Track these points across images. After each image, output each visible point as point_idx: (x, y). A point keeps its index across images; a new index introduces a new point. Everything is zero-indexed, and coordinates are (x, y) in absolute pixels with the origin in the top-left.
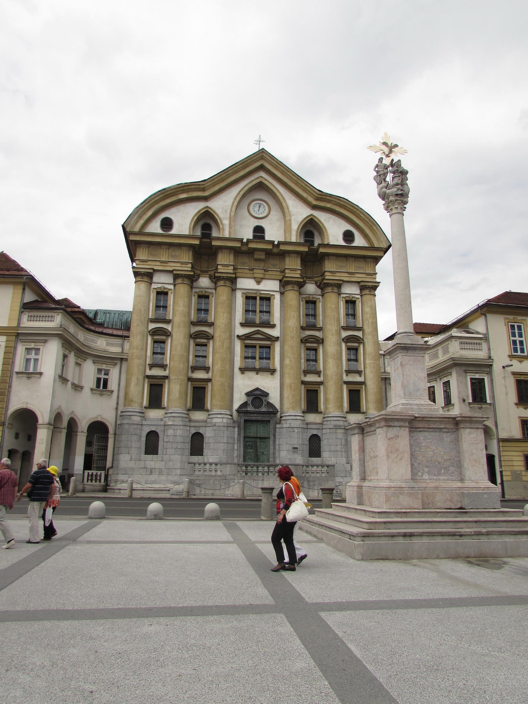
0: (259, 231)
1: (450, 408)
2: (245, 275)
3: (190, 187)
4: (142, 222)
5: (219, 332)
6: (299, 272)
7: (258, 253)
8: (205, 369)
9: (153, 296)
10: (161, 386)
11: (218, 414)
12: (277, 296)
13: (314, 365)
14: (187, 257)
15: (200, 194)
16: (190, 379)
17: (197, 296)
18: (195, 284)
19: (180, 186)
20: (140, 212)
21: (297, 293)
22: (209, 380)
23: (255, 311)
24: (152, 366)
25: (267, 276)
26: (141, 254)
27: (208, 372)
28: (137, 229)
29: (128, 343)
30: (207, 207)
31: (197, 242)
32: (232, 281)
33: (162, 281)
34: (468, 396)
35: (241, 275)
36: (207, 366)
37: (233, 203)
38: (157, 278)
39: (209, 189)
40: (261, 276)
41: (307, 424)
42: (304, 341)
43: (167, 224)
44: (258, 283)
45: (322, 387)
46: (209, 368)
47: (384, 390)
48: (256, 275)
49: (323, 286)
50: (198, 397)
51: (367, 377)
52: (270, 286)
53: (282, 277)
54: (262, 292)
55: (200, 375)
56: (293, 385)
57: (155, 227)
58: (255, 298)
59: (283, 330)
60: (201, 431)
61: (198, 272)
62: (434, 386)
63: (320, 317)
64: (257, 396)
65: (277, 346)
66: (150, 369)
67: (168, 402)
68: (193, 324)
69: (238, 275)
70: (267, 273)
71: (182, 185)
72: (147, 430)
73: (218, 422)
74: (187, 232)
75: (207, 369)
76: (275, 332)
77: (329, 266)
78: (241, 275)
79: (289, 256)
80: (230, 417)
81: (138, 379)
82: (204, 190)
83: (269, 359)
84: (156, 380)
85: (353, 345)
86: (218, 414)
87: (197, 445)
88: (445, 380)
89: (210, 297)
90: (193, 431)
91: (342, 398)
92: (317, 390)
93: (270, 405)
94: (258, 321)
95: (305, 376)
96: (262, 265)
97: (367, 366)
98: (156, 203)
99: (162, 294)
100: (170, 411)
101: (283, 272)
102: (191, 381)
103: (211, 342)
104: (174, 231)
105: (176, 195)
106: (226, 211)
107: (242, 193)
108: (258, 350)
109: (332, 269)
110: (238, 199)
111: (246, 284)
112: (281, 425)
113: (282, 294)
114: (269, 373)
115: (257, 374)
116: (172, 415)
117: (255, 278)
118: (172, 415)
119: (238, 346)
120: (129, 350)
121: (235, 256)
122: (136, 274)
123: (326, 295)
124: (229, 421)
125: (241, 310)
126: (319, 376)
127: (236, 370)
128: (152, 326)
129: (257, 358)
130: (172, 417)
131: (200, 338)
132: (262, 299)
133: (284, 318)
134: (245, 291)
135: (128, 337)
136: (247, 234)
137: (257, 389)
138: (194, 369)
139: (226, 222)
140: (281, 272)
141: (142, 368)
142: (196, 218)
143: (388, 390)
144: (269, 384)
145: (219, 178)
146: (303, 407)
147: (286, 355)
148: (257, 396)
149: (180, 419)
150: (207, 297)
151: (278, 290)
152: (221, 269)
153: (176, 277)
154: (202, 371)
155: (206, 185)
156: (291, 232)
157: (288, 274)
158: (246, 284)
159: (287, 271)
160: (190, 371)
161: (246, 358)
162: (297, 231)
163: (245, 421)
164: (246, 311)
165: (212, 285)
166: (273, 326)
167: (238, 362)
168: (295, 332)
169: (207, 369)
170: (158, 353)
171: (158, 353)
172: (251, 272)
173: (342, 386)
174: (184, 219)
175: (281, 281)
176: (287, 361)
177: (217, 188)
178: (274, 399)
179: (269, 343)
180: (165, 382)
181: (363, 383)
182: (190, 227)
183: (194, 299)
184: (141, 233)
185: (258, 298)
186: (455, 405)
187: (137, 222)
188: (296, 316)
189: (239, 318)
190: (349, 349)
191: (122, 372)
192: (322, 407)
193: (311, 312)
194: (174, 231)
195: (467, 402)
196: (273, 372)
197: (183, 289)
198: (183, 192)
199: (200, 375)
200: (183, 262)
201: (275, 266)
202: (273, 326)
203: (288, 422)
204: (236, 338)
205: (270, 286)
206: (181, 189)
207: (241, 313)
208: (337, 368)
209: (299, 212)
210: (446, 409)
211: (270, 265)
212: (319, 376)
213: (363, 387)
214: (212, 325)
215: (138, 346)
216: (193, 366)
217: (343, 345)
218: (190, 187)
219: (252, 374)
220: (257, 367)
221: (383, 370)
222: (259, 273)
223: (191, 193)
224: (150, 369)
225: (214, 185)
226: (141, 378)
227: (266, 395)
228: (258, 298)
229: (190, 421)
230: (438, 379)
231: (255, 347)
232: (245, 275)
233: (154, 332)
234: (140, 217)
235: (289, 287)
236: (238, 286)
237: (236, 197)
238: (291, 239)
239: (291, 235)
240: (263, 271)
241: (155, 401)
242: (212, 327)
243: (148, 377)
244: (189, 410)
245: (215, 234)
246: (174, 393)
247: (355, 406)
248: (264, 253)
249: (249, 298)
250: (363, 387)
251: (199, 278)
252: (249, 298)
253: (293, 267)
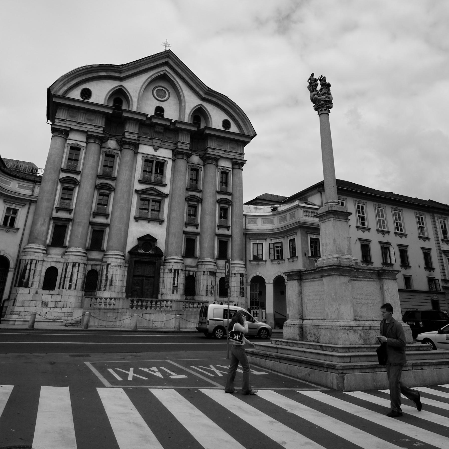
0: (160, 111)
1: (295, 259)
2: (146, 143)
3: (110, 68)
4: (65, 88)
6: (188, 146)
7: (156, 127)
8: (105, 216)
10: (65, 228)
11: (113, 254)
12: (170, 163)
13: (193, 219)
15: (117, 75)
16: (91, 223)
17: (104, 155)
18: (104, 145)
19: (101, 65)
20: (65, 80)
21: (186, 162)
22: (107, 225)
23: (151, 172)
24: (58, 210)
25: (163, 146)
26: (61, 115)
27: (107, 218)
28: (60, 93)
29: (39, 188)
30: (121, 86)
32: (135, 146)
33: (76, 138)
34: (308, 251)
35: (143, 142)
36: (107, 213)
37: (142, 86)
39: (124, 72)
40: (159, 145)
41: (186, 266)
42: (188, 199)
43: (86, 93)
44: (156, 150)
45: (198, 237)
46: (109, 214)
47: (244, 242)
48: (154, 144)
49: (206, 159)
51: (234, 233)
53: (175, 148)
54: (158, 158)
55: (101, 220)
56: (177, 234)
57: (76, 94)
58: (152, 162)
59: (172, 189)
60: (98, 268)
61: (107, 135)
62: (281, 243)
63: (201, 182)
64: (147, 241)
65: (166, 202)
66: (57, 212)
67: (70, 241)
68: (99, 177)
69: (140, 142)
70: (163, 143)
71: (103, 65)
72: (48, 265)
75: (106, 216)
76: (166, 190)
77: (211, 144)
78: (143, 142)
79: (182, 133)
80: (123, 258)
81: (44, 220)
82: (120, 72)
83: (159, 211)
84: (61, 222)
85: (225, 207)
86: (113, 254)
88: (292, 238)
89: (116, 157)
90: (89, 268)
91: (214, 247)
92: (195, 239)
93: (158, 249)
94: (153, 180)
95: (186, 227)
96: (160, 136)
97: (234, 223)
98: (80, 75)
100: (71, 250)
101: (176, 144)
102: (92, 225)
103: (113, 194)
104: (91, 100)
105: (97, 72)
106: (136, 91)
107: (150, 80)
109: (213, 147)
110: (146, 83)
111: (146, 149)
112: (165, 267)
113: (174, 161)
114: (158, 223)
115: (149, 223)
116: (73, 253)
117: (153, 146)
118: (73, 253)
119: (135, 199)
120: (39, 193)
121: (140, 128)
122: (54, 130)
123: (208, 166)
124: (122, 261)
125: (140, 170)
126: (197, 228)
127: (132, 218)
129: (150, 210)
132: (157, 163)
133: (174, 180)
134: (145, 155)
135: (40, 182)
136: (151, 112)
137: (148, 235)
138: (95, 215)
140: (174, 144)
141: (49, 210)
142: (111, 92)
143: (247, 243)
144: (158, 232)
145: (134, 65)
146: (183, 253)
147: (173, 209)
148: (147, 241)
149: (80, 257)
150: (113, 156)
151: (171, 157)
154: (103, 217)
155: (123, 69)
156: (184, 115)
157: (180, 146)
158: (146, 149)
159: (179, 144)
160: (92, 216)
161: (140, 209)
162: (189, 115)
163: (136, 262)
164: (144, 171)
165: (118, 147)
166: (165, 185)
167: (134, 212)
168: (181, 191)
169: (106, 216)
172: (151, 141)
173: (214, 238)
174: (101, 92)
175: (173, 151)
176: (174, 215)
178: (161, 244)
179: (160, 198)
180: (69, 224)
181: (230, 236)
182: (105, 98)
184: (63, 97)
185: (155, 162)
186: (299, 258)
187: (61, 88)
188: (183, 179)
189: (138, 176)
190: (221, 209)
191: (30, 212)
192: (197, 253)
193: (194, 178)
194: (91, 100)
195: (307, 255)
196: (161, 222)
198: (103, 71)
199: (101, 220)
201: (169, 138)
202: (165, 185)
203: (171, 264)
204: (134, 192)
205: (165, 154)
206: (102, 68)
207: (140, 172)
208: (212, 222)
210: (291, 260)
211: (166, 138)
212: (197, 228)
213: (230, 239)
214: (114, 179)
216: (96, 212)
217: (217, 205)
218: (110, 68)
219: (144, 223)
220: (149, 217)
221: (244, 227)
222: (157, 143)
223: (109, 73)
224: (57, 212)
226: (47, 219)
227: (155, 240)
228: (155, 162)
229: (88, 259)
230: (286, 237)
231: (148, 200)
232: (146, 143)
234: (64, 85)
235: (180, 157)
237: (145, 82)
238: (184, 120)
239: (184, 117)
240: (160, 142)
241: (58, 240)
242: (115, 181)
243: (54, 219)
244: (87, 250)
245: (124, 107)
247: (223, 254)
248: (163, 128)
249: (148, 161)
250: (230, 239)
251: (107, 140)
252: (148, 161)
253: (184, 142)
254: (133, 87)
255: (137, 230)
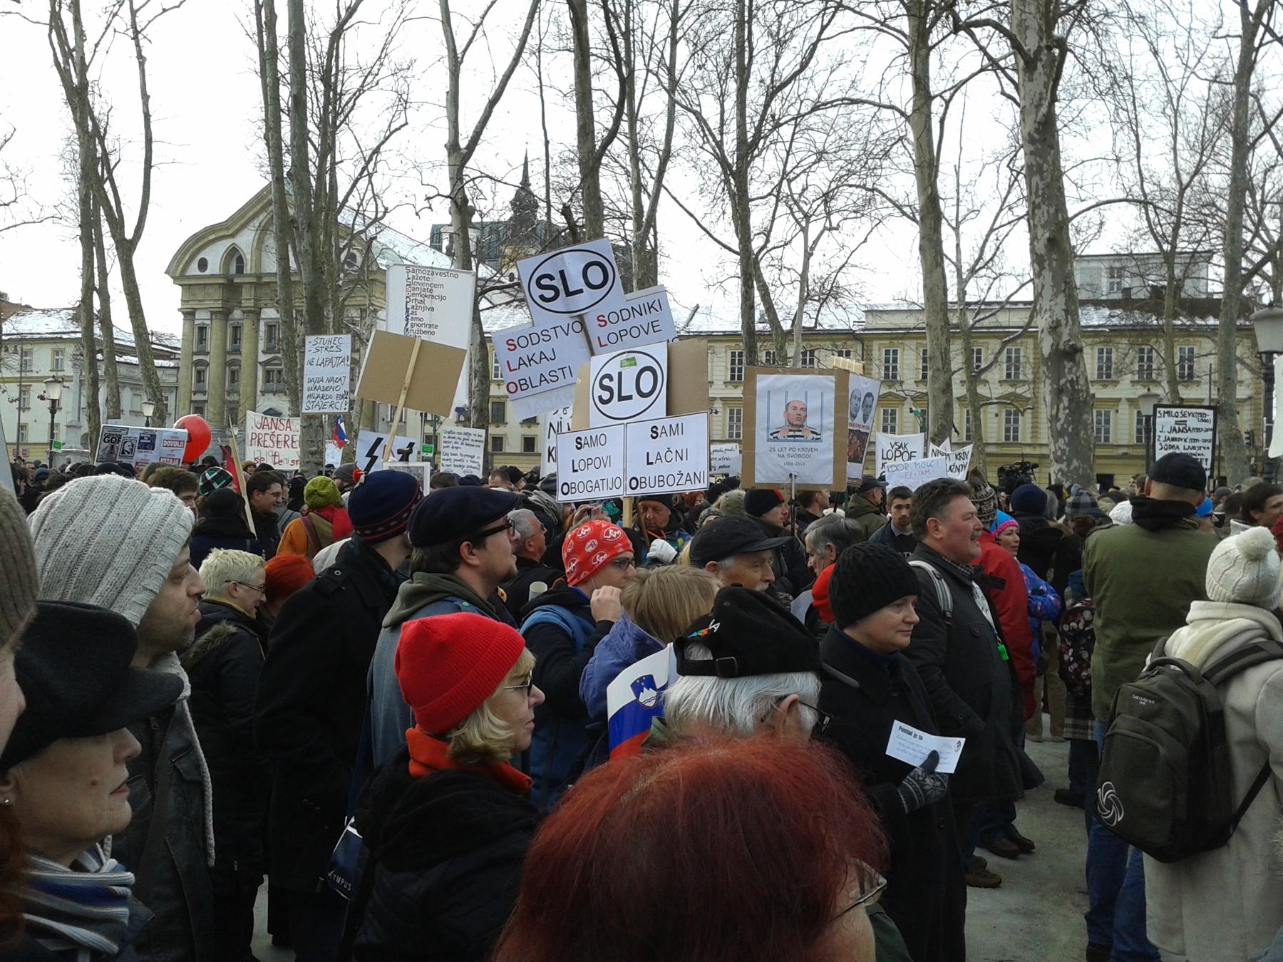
5: (245, 358)
9: (196, 331)
14: (217, 294)
15: (225, 233)
16: (224, 402)
31: (221, 281)
32: (256, 313)
38: (197, 316)
43: (203, 264)
55: (234, 397)
68: (229, 353)
74: (217, 272)
75: (238, 392)
82: (227, 229)
98: (190, 247)
99: (202, 329)
128: (195, 358)
139: (249, 257)
152: (245, 303)
153: (212, 313)
170: (200, 379)
171: (200, 379)
174: (215, 256)
177: (237, 226)
183: (229, 331)
197: (217, 325)
199: (234, 397)
200: (214, 300)
219: (271, 395)
225: (235, 223)
226: (187, 403)
233: (197, 363)
234: (179, 262)
236: (263, 316)
243: (192, 401)
254: (245, 241)
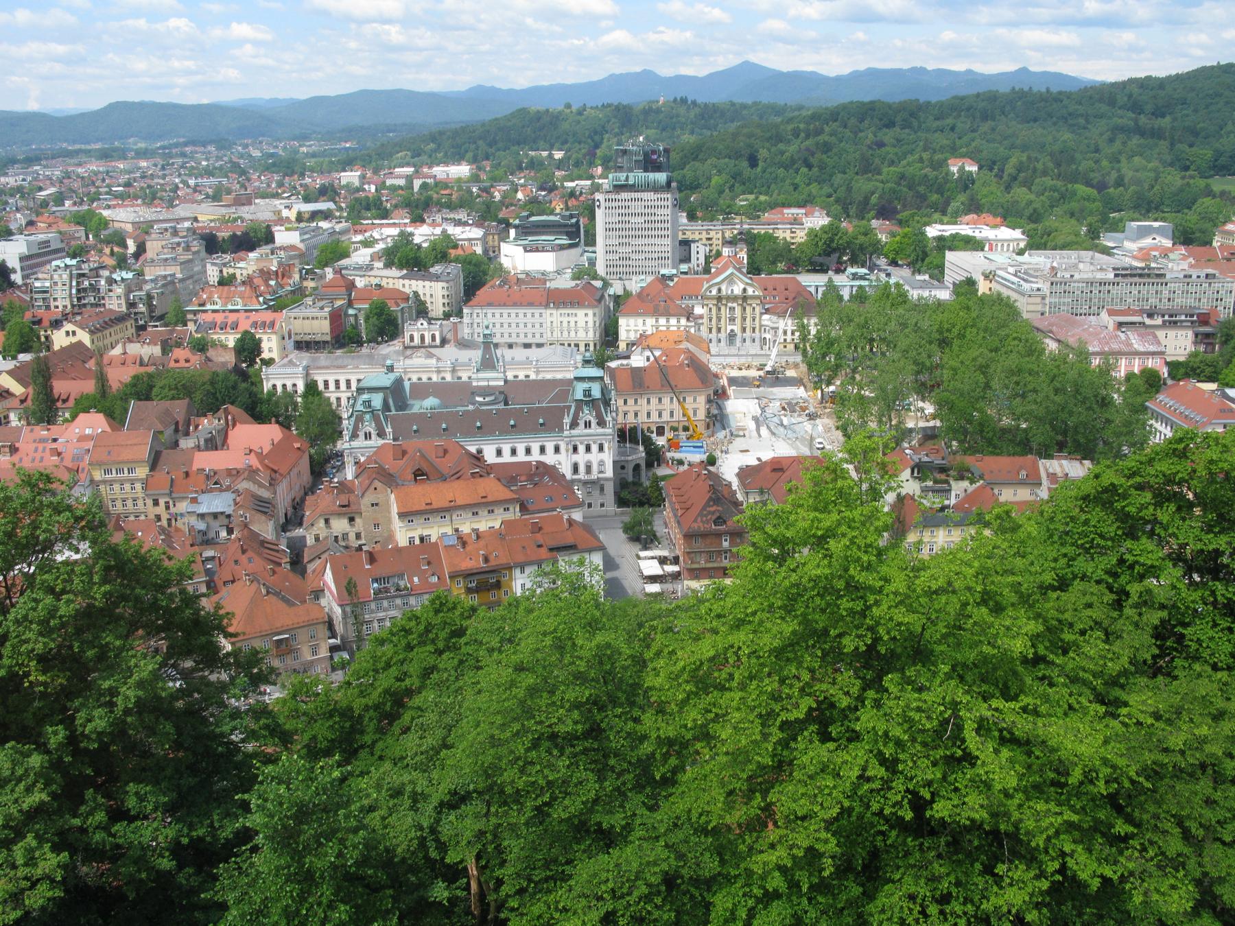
50: (719, 330)
52: (735, 305)
64: (732, 331)
73: (723, 335)
87: (719, 341)
108: (732, 320)
130: (713, 336)
131: (719, 319)
133: (738, 311)
144: (734, 328)
147: (738, 321)
148: (732, 331)
158: (730, 305)
174: (714, 292)
209: (742, 286)
215: (705, 320)
246: (714, 330)
255: (729, 328)
